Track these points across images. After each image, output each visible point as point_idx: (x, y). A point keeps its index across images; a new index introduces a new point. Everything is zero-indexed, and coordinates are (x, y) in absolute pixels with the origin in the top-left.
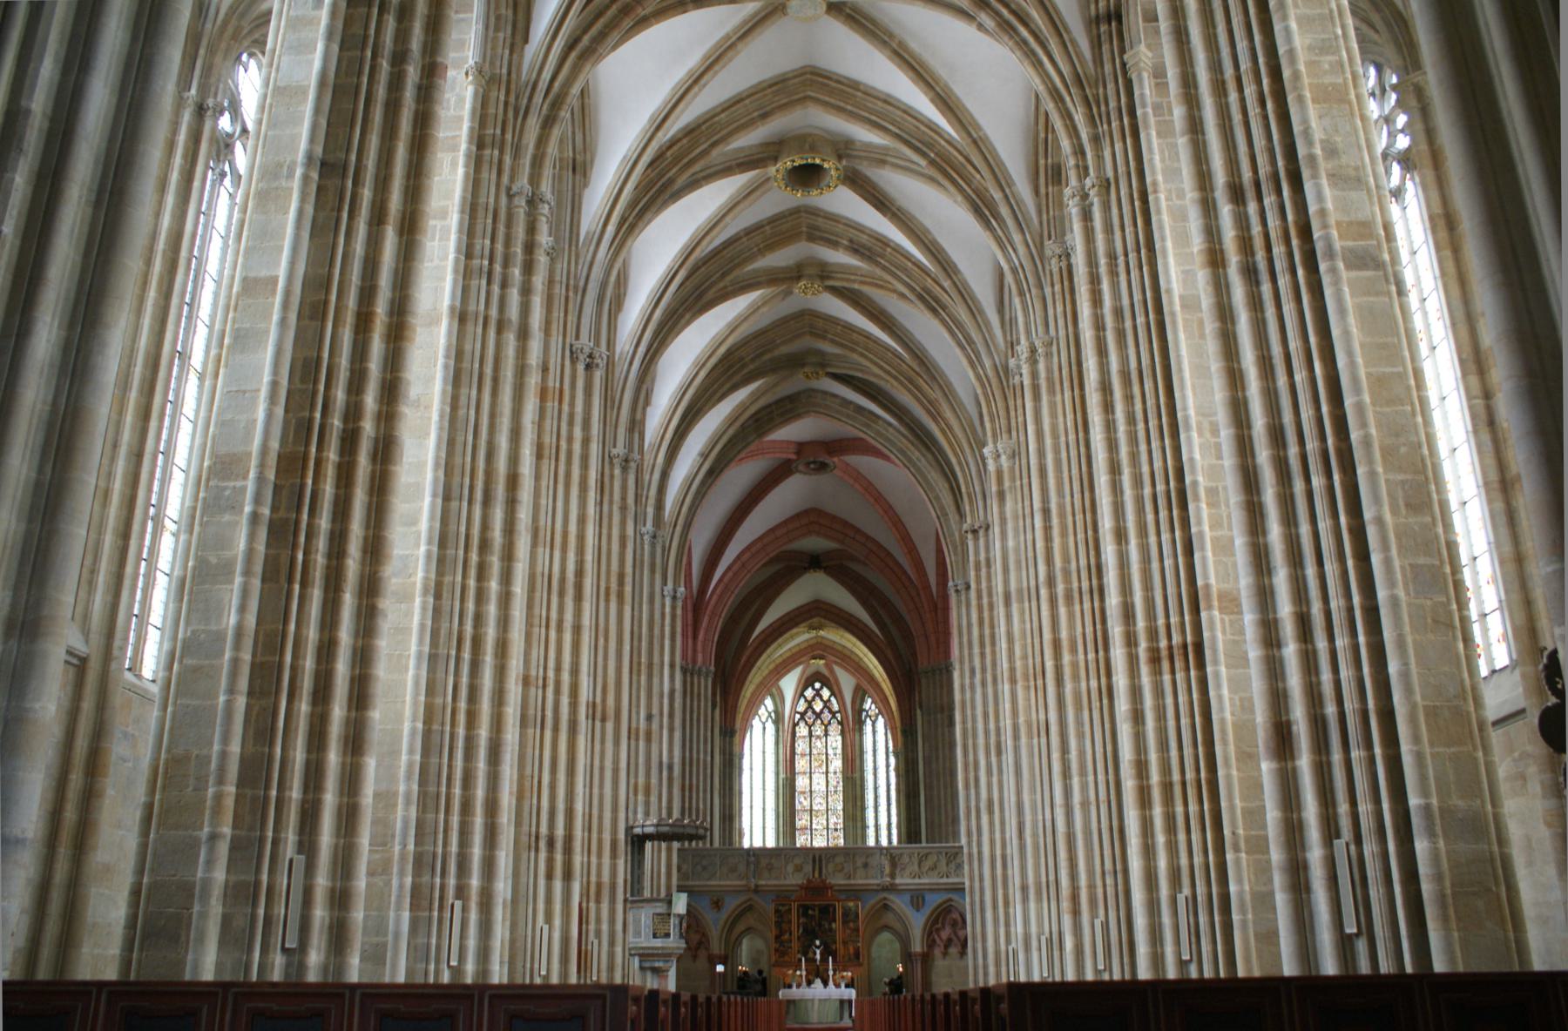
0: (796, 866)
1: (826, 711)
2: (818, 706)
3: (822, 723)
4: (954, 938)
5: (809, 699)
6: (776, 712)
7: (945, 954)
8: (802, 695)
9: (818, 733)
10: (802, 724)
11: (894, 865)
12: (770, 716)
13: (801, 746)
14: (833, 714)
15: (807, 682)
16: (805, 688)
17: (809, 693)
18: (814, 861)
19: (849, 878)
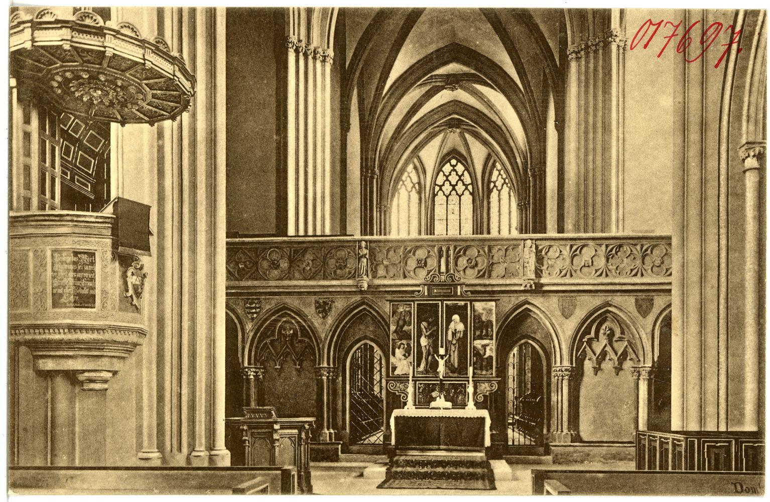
0: (419, 261)
1: (460, 183)
2: (454, 179)
3: (457, 194)
4: (608, 349)
5: (447, 174)
6: (419, 183)
7: (597, 370)
8: (440, 170)
9: (454, 202)
10: (440, 193)
11: (540, 260)
12: (414, 186)
13: (440, 211)
14: (466, 186)
15: (444, 160)
16: (444, 166)
17: (447, 168)
18: (440, 256)
19: (483, 276)
